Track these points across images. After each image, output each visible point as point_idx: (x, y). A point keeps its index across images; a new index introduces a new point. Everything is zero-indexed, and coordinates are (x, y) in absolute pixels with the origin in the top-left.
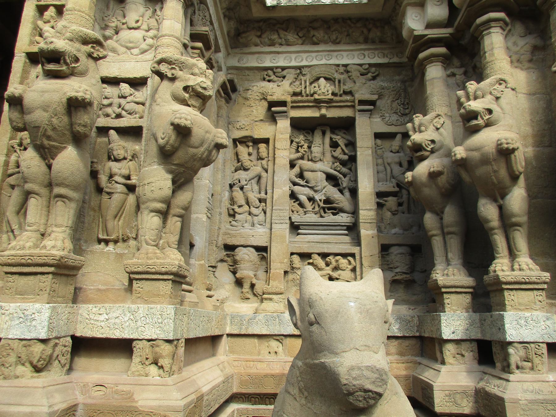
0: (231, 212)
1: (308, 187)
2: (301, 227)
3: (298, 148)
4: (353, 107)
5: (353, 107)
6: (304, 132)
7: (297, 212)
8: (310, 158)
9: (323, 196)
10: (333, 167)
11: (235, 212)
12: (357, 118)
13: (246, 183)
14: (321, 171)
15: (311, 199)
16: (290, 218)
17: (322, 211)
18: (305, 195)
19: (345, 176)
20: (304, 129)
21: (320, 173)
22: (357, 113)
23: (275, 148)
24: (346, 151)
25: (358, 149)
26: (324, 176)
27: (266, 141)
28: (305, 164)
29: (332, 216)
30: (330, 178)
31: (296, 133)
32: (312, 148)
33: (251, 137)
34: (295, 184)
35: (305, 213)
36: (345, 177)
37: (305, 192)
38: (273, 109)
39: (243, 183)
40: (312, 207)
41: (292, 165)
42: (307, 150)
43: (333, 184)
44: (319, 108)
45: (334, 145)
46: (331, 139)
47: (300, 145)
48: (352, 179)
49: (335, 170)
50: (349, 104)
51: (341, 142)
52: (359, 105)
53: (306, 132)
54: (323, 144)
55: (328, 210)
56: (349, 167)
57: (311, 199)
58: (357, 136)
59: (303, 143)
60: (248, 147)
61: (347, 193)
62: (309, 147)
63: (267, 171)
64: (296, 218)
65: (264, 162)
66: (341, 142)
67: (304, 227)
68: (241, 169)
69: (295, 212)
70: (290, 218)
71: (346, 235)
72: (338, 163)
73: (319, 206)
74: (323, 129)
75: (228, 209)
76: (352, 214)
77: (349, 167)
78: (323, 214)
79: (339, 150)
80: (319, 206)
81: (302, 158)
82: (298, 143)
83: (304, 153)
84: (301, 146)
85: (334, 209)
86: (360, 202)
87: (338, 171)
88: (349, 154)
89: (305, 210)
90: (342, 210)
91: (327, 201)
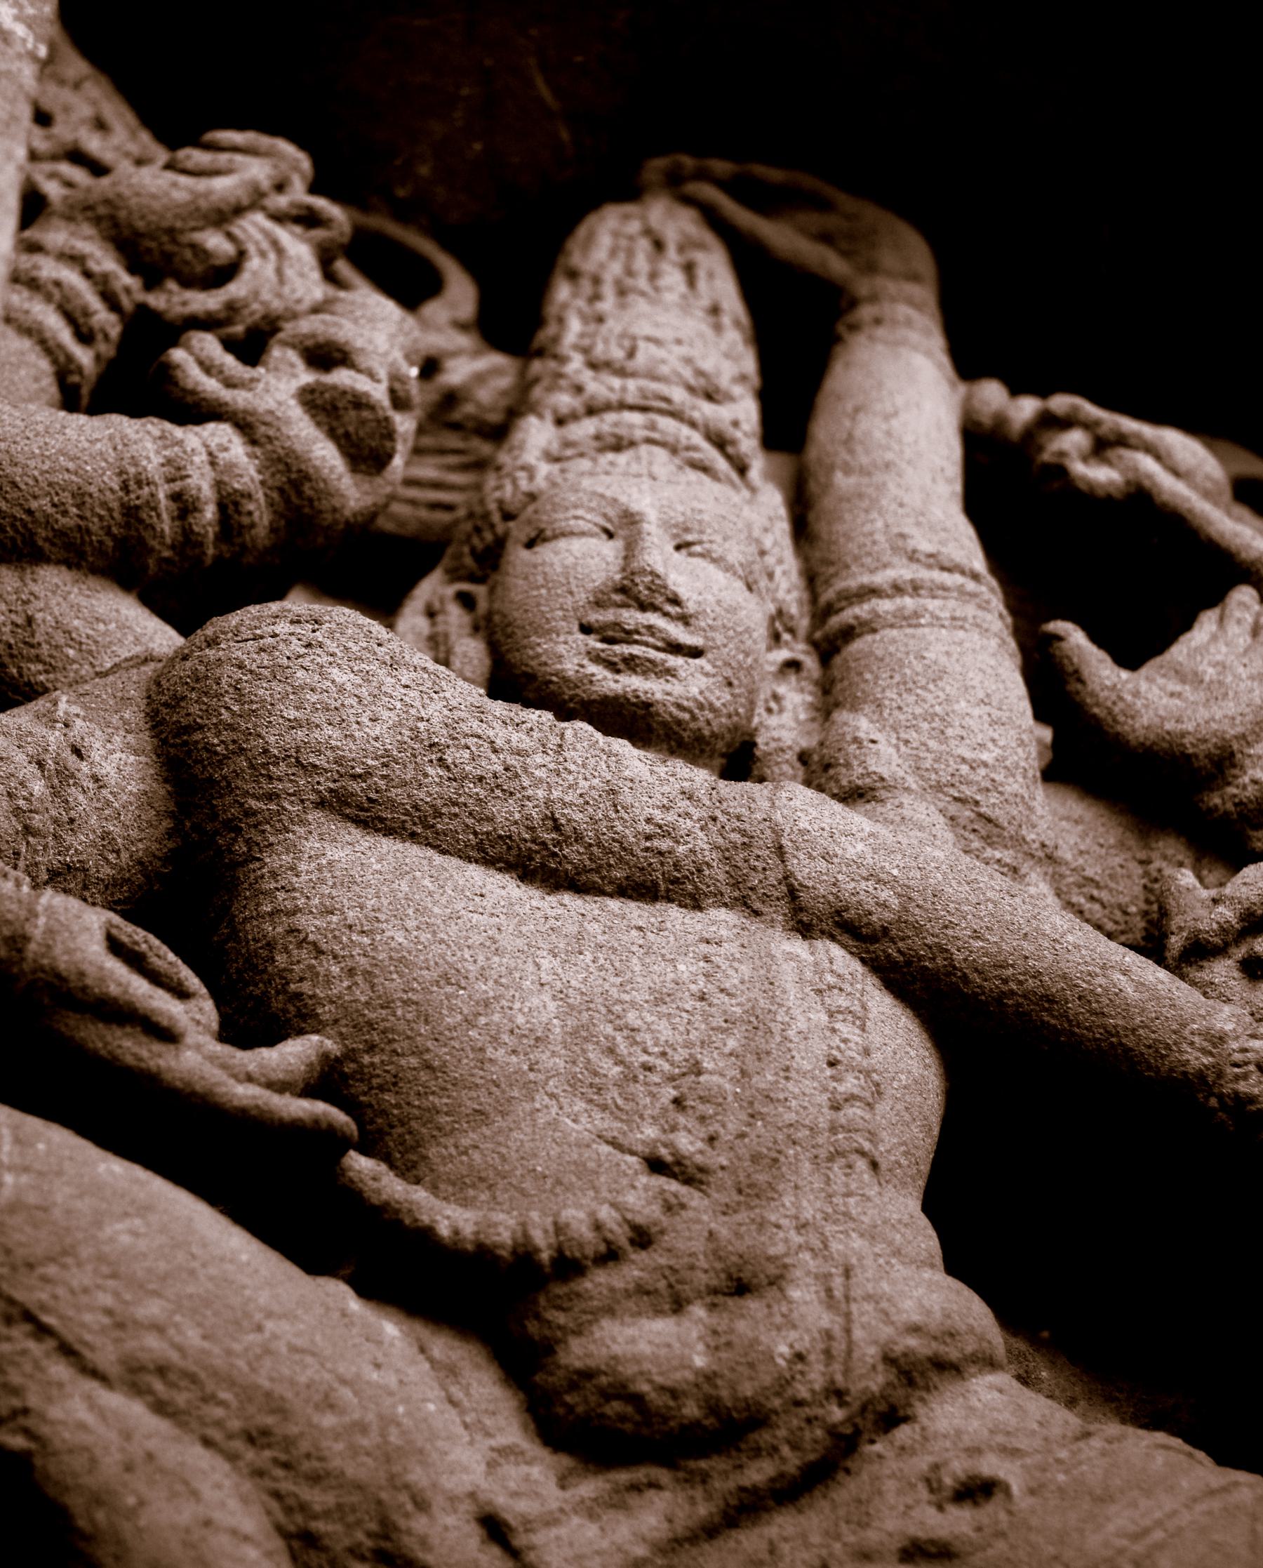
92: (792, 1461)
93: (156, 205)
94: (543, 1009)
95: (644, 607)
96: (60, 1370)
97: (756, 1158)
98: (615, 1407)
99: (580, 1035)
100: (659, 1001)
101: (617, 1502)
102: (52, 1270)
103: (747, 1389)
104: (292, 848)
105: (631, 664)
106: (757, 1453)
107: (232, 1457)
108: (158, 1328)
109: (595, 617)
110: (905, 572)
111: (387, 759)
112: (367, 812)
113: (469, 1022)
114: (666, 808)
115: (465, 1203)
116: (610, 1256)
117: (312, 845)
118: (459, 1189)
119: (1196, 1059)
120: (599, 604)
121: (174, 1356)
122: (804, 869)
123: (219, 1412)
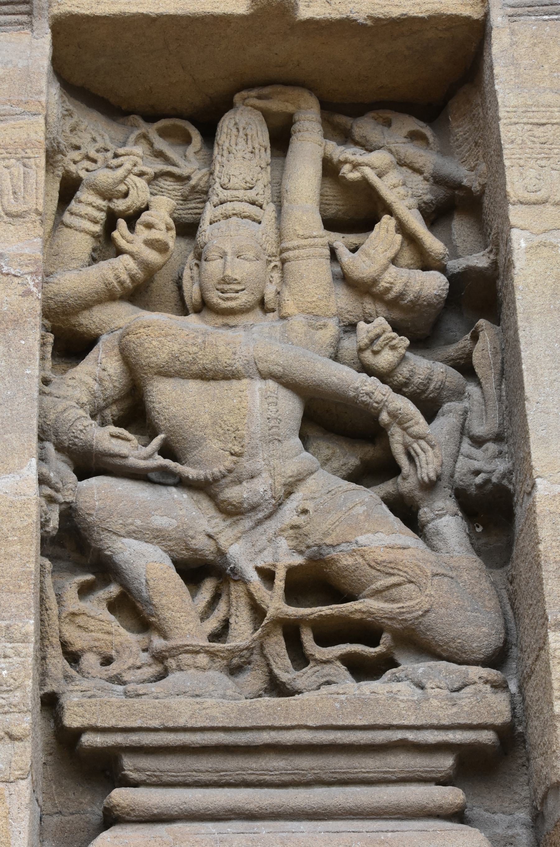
1: (183, 483)
2: (130, 765)
6: (151, 130)
7: (107, 661)
8: (192, 292)
9: (284, 544)
10: (349, 345)
12: (497, 19)
14: (265, 376)
15: (199, 570)
16: (50, 703)
17: (277, 646)
18: (157, 537)
19: (430, 409)
20: (151, 118)
21: (258, 384)
24: (433, 243)
25: (516, 215)
26: (290, 407)
28: (162, 332)
29: (349, 686)
30: (331, 420)
31: (94, 131)
32: (205, 225)
34: (88, 464)
35: (162, 663)
36: (430, 417)
37: (160, 521)
40: (212, 624)
41: (70, 344)
42: (170, 238)
43: (353, 461)
46: (330, 169)
47: (120, 205)
48: (479, 428)
49: (366, 369)
51: (402, 193)
54: (279, 202)
55: (323, 640)
56: (452, 350)
57: (199, 570)
58: (506, 132)
59: (140, 191)
61: (448, 523)
62: (187, 229)
64: (89, 707)
66: (402, 193)
67: (149, 763)
69: (90, 661)
70: (50, 703)
71: (458, 816)
72: (381, 323)
73: (257, 611)
74: (275, 105)
76: (485, 663)
77: (452, 350)
78: (285, 671)
79: (383, 238)
80: (257, 611)
81: (138, 293)
82: (107, 195)
83: (153, 256)
84: (132, 219)
85: (367, 632)
86: (549, 574)
87: (384, 377)
89: (158, 643)
90: (417, 642)
91: (315, 581)
92: (267, 512)
93: (105, 185)
94: (206, 419)
95: (229, 284)
96: (114, 537)
97: (252, 448)
98: (230, 507)
99: (215, 423)
100: (230, 412)
101: (235, 523)
102: (109, 520)
103: (255, 500)
104: (152, 385)
105: (228, 299)
106: (260, 511)
107: (152, 543)
108: (132, 524)
109: (220, 287)
110: (295, 243)
111: (167, 362)
112: (165, 373)
113: (190, 427)
114: (229, 359)
115: (195, 468)
116: (224, 476)
117: (155, 383)
118: (194, 464)
119: (352, 394)
120: (219, 283)
121: (136, 528)
122: (261, 366)
123: (148, 536)
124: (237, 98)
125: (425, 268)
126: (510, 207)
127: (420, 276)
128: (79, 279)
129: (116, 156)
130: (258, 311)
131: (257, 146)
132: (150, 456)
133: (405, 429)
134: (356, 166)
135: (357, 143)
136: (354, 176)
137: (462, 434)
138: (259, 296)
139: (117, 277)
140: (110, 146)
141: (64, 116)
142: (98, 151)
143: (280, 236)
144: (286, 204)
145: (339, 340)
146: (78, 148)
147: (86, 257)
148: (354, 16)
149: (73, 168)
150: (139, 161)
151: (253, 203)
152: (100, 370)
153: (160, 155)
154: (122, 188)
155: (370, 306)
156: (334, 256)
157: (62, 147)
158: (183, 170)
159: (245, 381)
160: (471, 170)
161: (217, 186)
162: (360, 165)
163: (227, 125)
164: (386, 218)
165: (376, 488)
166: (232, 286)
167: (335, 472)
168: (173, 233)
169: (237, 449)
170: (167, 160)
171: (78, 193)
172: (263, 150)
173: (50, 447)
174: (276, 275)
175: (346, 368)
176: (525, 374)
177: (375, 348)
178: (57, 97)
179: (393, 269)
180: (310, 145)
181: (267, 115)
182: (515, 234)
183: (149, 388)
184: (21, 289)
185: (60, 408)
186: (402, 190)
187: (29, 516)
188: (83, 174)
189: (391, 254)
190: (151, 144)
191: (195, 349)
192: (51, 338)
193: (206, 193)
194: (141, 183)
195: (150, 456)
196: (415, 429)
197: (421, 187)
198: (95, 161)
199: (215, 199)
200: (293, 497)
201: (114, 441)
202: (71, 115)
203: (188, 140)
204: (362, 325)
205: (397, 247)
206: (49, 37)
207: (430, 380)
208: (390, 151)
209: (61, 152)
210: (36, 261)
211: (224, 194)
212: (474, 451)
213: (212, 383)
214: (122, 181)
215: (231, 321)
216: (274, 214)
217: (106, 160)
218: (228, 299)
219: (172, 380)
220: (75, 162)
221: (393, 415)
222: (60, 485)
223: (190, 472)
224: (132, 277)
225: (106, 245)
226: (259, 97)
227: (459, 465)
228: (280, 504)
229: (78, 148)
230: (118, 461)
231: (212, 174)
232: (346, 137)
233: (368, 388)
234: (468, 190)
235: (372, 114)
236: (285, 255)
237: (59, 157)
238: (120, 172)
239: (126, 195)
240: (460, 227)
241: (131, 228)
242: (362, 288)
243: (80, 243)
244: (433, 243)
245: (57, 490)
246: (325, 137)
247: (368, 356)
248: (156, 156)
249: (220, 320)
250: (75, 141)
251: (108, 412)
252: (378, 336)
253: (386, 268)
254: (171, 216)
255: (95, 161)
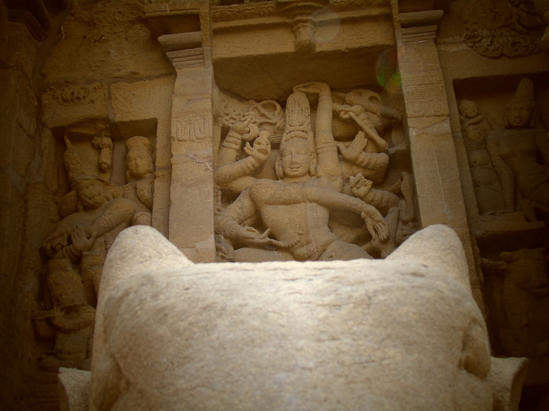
0: (44, 330)
3: (243, 145)
4: (388, 17)
5: (388, 17)
6: (259, 105)
8: (279, 171)
10: (347, 187)
11: (56, 329)
13: (89, 242)
14: (311, 201)
19: (384, 211)
22: (399, 32)
23: (169, 138)
26: (323, 214)
27: (148, 129)
28: (266, 188)
31: (234, 107)
32: (283, 142)
33: (106, 120)
38: (162, 38)
39: (81, 242)
41: (228, 196)
44: (292, 28)
45: (347, 131)
46: (336, 115)
47: (246, 136)
48: (404, 217)
49: (355, 196)
50: (375, 12)
51: (368, 123)
52: (400, 12)
53: (264, 106)
54: (314, 130)
59: (254, 130)
60: (98, 149)
62: (276, 146)
63: (150, 209)
65: (143, 186)
68: (76, 210)
72: (360, 175)
74: (311, 90)
75: (33, 322)
77: (393, 187)
79: (360, 140)
87: (362, 198)
88: (392, 151)
105: (294, 171)
110: (321, 146)
112: (268, 203)
116: (296, 244)
119: (348, 205)
122: (309, 197)
124: (294, 88)
125: (379, 152)
126: (408, 119)
127: (376, 155)
128: (230, 167)
129: (244, 116)
130: (308, 175)
131: (303, 107)
132: (264, 238)
133: (372, 219)
134: (346, 112)
135: (348, 104)
136: (345, 116)
137: (398, 220)
138: (307, 169)
139: (247, 166)
140: (241, 113)
141: (221, 102)
142: (236, 115)
143: (315, 144)
144: (317, 130)
145: (343, 186)
146: (228, 114)
147: (234, 159)
148: (340, 48)
149: (226, 123)
150: (254, 117)
151: (303, 131)
152: (242, 205)
153: (263, 115)
154: (247, 129)
155: (355, 170)
156: (339, 152)
157: (221, 114)
158: (273, 121)
159: (303, 204)
160: (397, 110)
161: (288, 125)
162: (348, 111)
163: (290, 100)
164: (360, 132)
165: (363, 247)
166: (295, 166)
167: (345, 241)
168: (269, 146)
169: (301, 232)
170: (266, 117)
171: (229, 133)
172: (306, 110)
173: (222, 237)
174: (315, 161)
175: (346, 195)
176: (417, 186)
177: (358, 186)
178: (217, 93)
179: (364, 153)
180: (327, 105)
181: (308, 95)
182: (411, 130)
183: (262, 210)
184: (204, 168)
185: (225, 220)
186: (367, 121)
187: (212, 257)
188: (230, 125)
189: (363, 147)
190: (259, 111)
191: (281, 192)
192: (220, 193)
193: (283, 129)
194: (255, 126)
195: (264, 238)
196: (377, 218)
197: (376, 119)
198: (235, 119)
199: (287, 131)
200: (326, 251)
201: (248, 232)
202: (224, 101)
203: (275, 109)
204: (352, 178)
205: (365, 144)
206: (212, 67)
207: (382, 198)
208: (362, 105)
209: (220, 116)
210: (210, 157)
211: (291, 129)
212: (405, 227)
213: (289, 206)
214: (247, 126)
215: (296, 180)
216: (312, 136)
217: (240, 118)
218: (294, 171)
219: (272, 206)
220: (227, 121)
221: (367, 213)
222: (226, 252)
223: (281, 244)
224: (253, 166)
225: (242, 154)
226: (304, 87)
227: (398, 233)
228: (321, 255)
229: (228, 114)
230: (250, 240)
231: (285, 121)
232: (343, 102)
233: (355, 203)
234: (396, 119)
235: (354, 91)
236: (318, 151)
237: (220, 118)
238: (246, 123)
239: (249, 132)
240: (395, 136)
241: (252, 145)
242: (351, 162)
243: (231, 152)
244: (381, 141)
245: (225, 254)
246: (334, 102)
247: (355, 190)
248: (262, 116)
249: (292, 180)
250: (226, 112)
251: (246, 222)
252: (359, 181)
253: (361, 153)
254: (268, 139)
255: (235, 119)
